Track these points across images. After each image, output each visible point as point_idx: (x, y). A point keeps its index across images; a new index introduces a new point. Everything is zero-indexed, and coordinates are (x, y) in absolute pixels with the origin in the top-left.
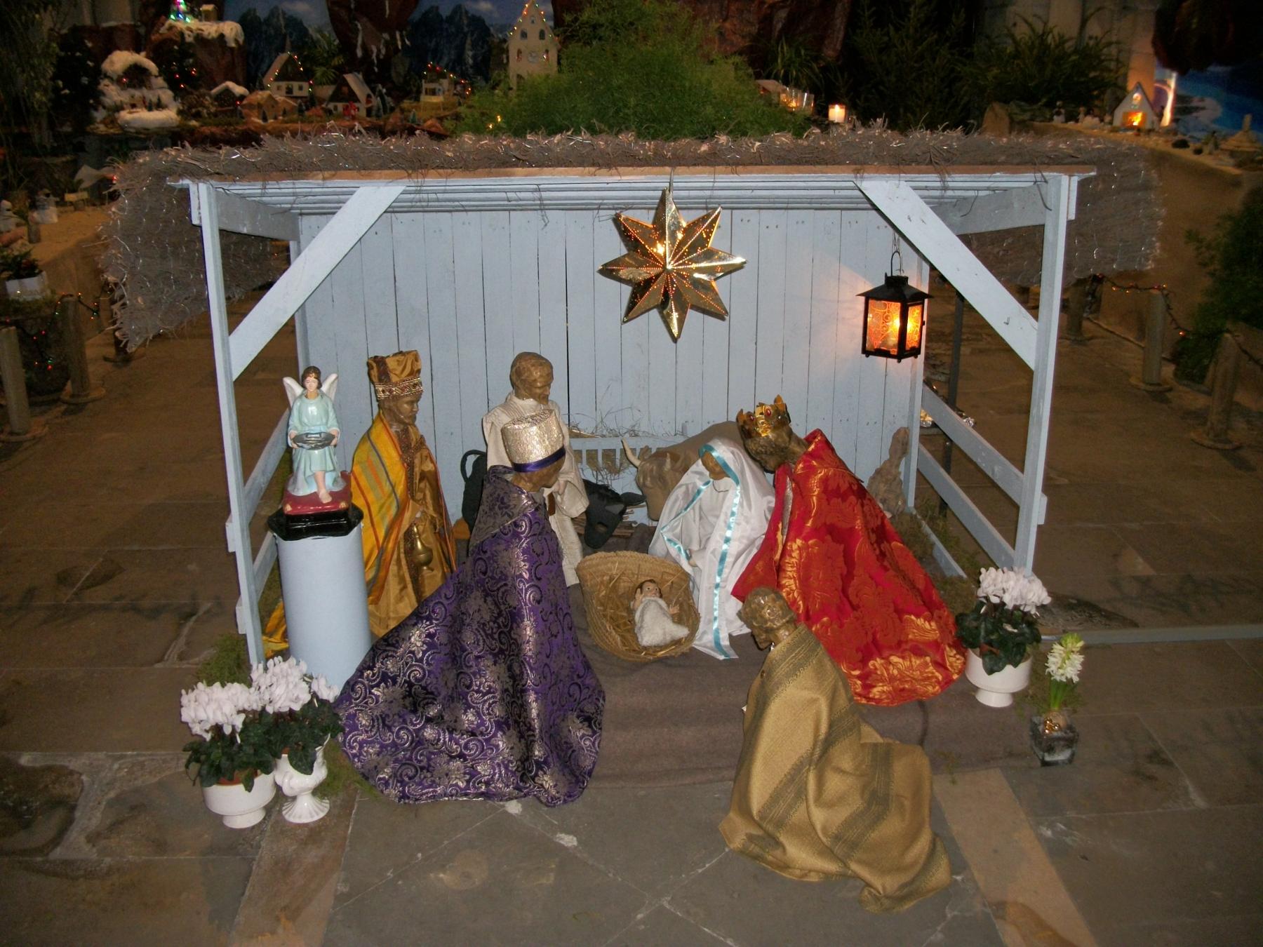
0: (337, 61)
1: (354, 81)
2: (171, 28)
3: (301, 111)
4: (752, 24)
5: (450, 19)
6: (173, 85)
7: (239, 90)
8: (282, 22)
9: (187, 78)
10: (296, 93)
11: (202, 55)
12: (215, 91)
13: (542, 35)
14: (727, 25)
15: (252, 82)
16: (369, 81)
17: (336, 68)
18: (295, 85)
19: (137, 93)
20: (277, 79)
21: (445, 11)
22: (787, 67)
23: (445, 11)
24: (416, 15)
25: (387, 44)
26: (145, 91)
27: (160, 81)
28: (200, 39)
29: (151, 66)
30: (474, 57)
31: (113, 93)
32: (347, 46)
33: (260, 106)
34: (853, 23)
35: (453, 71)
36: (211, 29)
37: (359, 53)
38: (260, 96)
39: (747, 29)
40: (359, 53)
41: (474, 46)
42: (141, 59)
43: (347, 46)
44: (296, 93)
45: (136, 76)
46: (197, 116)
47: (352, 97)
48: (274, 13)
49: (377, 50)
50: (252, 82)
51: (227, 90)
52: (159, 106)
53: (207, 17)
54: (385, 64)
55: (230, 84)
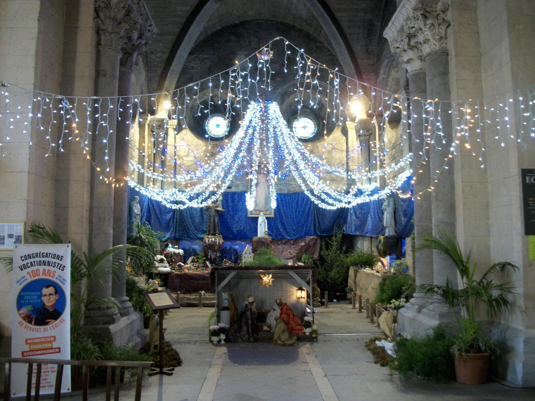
0: (204, 258)
1: (207, 263)
2: (168, 251)
3: (197, 269)
4: (297, 250)
5: (229, 250)
6: (169, 263)
7: (182, 264)
8: (191, 250)
9: (172, 261)
10: (195, 265)
11: (175, 257)
12: (178, 264)
13: (250, 254)
14: (291, 251)
15: (185, 262)
16: (211, 263)
17: (204, 260)
18: (194, 263)
19: (161, 264)
20: (191, 262)
21: (228, 248)
22: (304, 260)
23: (228, 248)
24: (221, 249)
25: (215, 255)
26: (163, 264)
27: (166, 262)
28: (175, 253)
29: (165, 259)
30: (234, 258)
31: (157, 264)
32: (206, 255)
33: (187, 268)
34: (321, 249)
35: (229, 261)
36: (177, 251)
37: (209, 257)
38: (187, 266)
39: (296, 251)
40: (209, 257)
41: (234, 255)
42: (163, 257)
43: (206, 255)
44: (195, 265)
45: (161, 261)
46: (174, 270)
47: (207, 266)
48: (190, 248)
49: (213, 257)
50: (185, 262)
51: (180, 265)
52: (166, 267)
53: (176, 248)
54: (215, 259)
55: (181, 263)
